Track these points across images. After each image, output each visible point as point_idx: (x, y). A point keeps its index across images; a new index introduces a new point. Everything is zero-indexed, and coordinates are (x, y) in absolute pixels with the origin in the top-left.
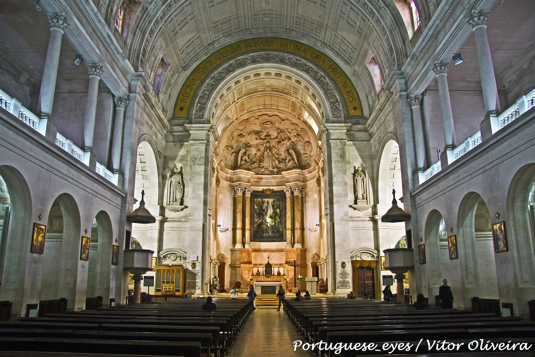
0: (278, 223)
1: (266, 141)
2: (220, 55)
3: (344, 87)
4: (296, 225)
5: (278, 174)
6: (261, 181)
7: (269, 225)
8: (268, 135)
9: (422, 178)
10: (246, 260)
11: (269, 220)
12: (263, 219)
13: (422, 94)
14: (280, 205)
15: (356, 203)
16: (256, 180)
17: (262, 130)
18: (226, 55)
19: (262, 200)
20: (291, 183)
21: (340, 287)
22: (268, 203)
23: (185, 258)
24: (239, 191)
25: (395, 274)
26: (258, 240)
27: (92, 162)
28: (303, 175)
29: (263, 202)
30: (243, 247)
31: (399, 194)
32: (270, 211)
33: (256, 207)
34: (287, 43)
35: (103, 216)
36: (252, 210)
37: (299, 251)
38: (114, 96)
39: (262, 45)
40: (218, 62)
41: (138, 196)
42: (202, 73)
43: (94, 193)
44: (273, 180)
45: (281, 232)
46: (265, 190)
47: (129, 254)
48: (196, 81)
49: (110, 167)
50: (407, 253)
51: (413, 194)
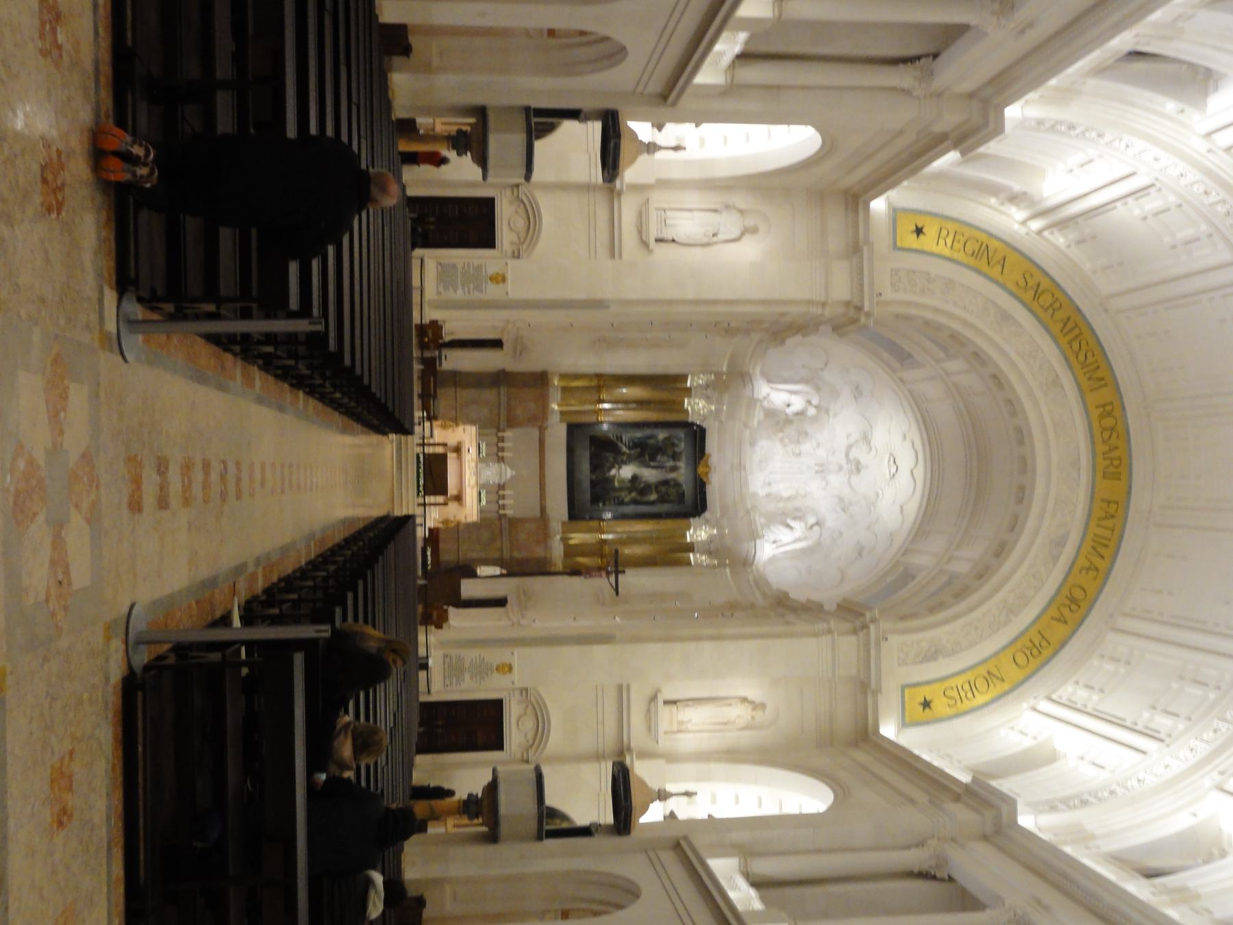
0: (618, 498)
1: (843, 461)
2: (1076, 332)
3: (986, 675)
7: (613, 472)
8: (858, 467)
9: (723, 868)
10: (519, 412)
11: (626, 472)
12: (629, 456)
13: (951, 879)
14: (668, 501)
15: (666, 702)
17: (874, 451)
18: (1076, 346)
19: (681, 453)
21: (447, 660)
22: (674, 469)
23: (516, 255)
25: (480, 795)
27: (747, 23)
29: (675, 457)
31: (685, 810)
32: (649, 475)
34: (1113, 517)
35: (616, 54)
38: (935, 56)
39: (1106, 448)
40: (1056, 329)
41: (673, 132)
42: (1022, 283)
43: (668, 32)
46: (707, 461)
47: (521, 121)
48: (1000, 268)
49: (744, 57)
50: (533, 825)
51: (683, 843)
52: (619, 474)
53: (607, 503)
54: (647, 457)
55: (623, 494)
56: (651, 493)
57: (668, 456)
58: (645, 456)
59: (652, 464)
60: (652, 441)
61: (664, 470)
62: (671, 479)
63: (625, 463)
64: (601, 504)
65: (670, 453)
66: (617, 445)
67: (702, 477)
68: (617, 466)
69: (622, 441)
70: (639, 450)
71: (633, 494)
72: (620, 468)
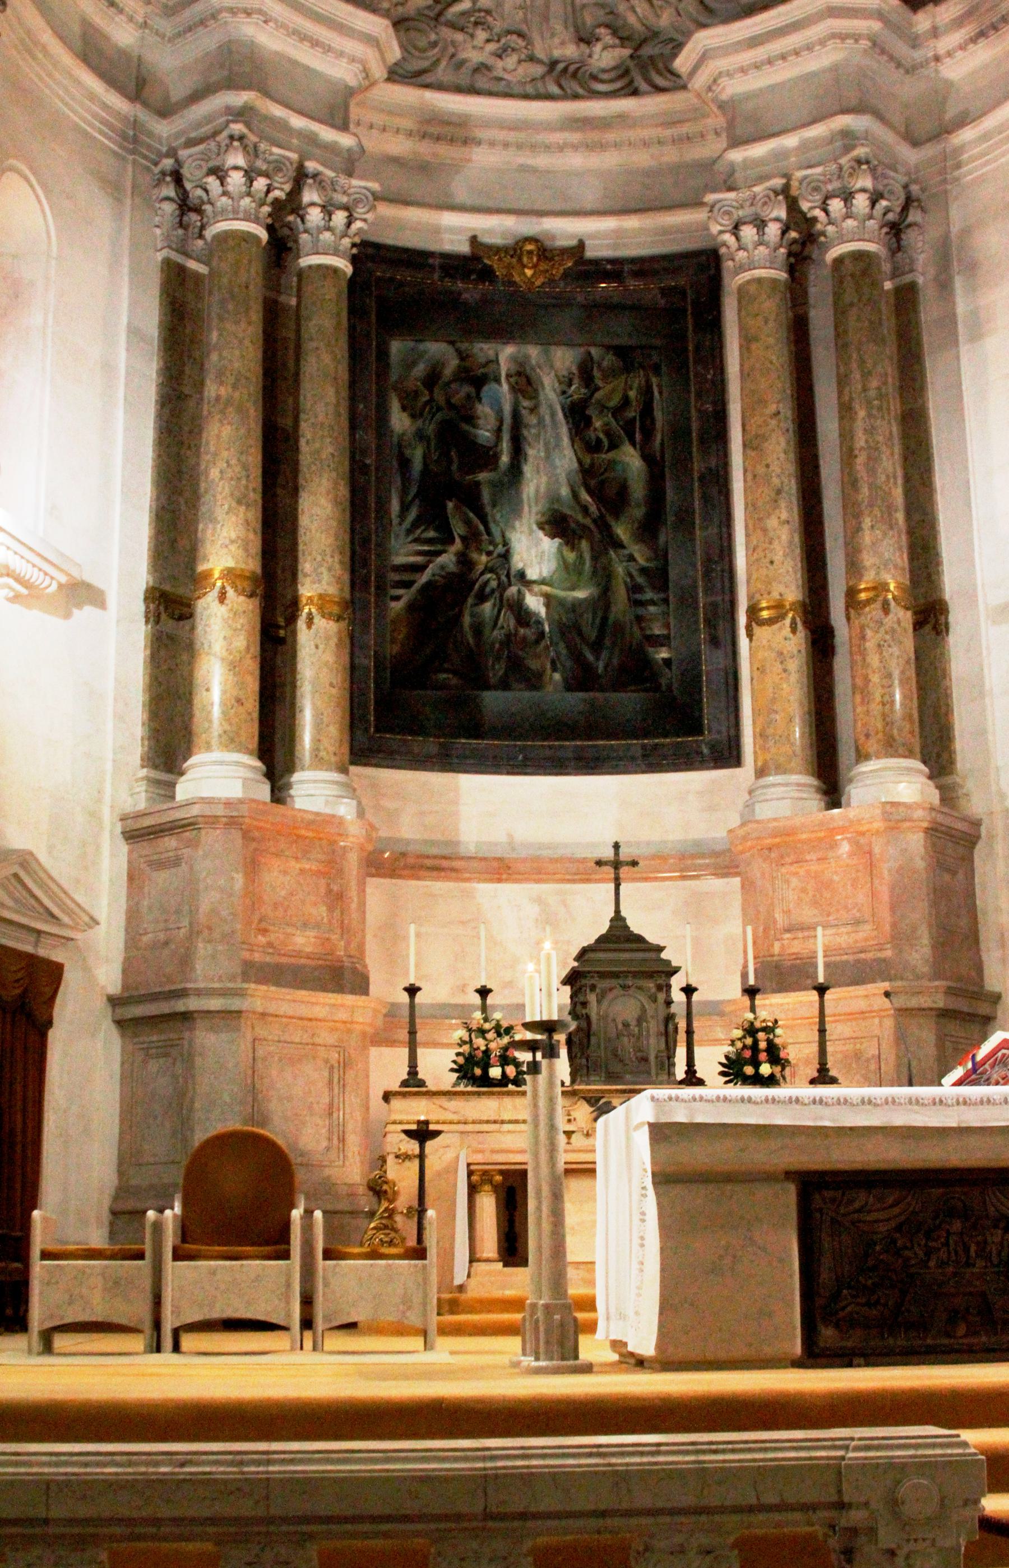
0: (635, 588)
4: (868, 559)
5: (635, 93)
6: (455, 168)
7: (534, 603)
14: (647, 410)
16: (399, 146)
19: (463, 356)
20: (790, 141)
24: (236, 180)
26: (431, 745)
28: (911, 70)
30: (264, 791)
33: (400, 421)
36: (368, 438)
37: (916, 842)
44: (576, 161)
45: (669, 678)
52: (543, 582)
53: (657, 630)
54: (483, 476)
55: (620, 570)
56: (612, 464)
57: (480, 400)
58: (478, 484)
59: (505, 459)
60: (417, 455)
61: (533, 420)
62: (564, 393)
63: (506, 556)
64: (664, 654)
65: (467, 389)
66: (429, 584)
67: (558, 272)
68: (513, 590)
69: (420, 568)
70: (450, 505)
71: (621, 531)
72: (522, 575)
